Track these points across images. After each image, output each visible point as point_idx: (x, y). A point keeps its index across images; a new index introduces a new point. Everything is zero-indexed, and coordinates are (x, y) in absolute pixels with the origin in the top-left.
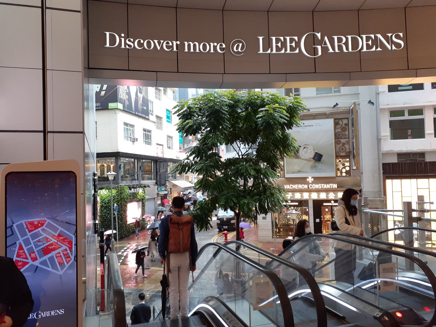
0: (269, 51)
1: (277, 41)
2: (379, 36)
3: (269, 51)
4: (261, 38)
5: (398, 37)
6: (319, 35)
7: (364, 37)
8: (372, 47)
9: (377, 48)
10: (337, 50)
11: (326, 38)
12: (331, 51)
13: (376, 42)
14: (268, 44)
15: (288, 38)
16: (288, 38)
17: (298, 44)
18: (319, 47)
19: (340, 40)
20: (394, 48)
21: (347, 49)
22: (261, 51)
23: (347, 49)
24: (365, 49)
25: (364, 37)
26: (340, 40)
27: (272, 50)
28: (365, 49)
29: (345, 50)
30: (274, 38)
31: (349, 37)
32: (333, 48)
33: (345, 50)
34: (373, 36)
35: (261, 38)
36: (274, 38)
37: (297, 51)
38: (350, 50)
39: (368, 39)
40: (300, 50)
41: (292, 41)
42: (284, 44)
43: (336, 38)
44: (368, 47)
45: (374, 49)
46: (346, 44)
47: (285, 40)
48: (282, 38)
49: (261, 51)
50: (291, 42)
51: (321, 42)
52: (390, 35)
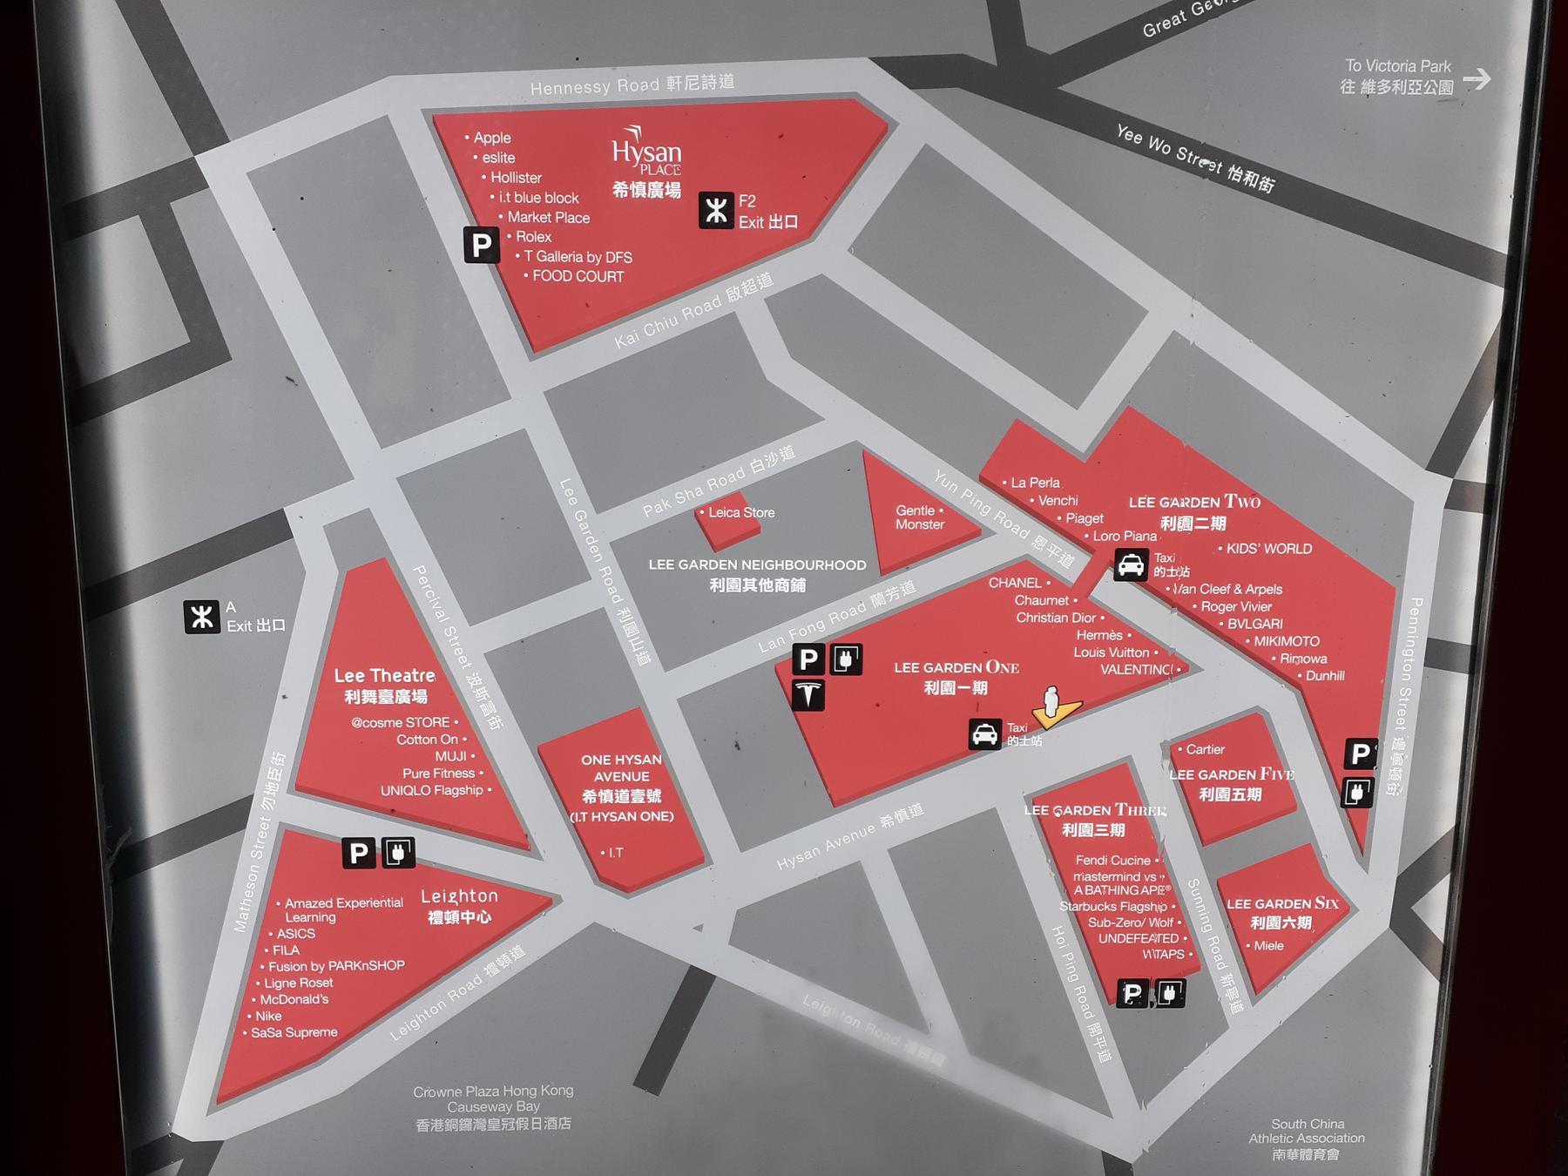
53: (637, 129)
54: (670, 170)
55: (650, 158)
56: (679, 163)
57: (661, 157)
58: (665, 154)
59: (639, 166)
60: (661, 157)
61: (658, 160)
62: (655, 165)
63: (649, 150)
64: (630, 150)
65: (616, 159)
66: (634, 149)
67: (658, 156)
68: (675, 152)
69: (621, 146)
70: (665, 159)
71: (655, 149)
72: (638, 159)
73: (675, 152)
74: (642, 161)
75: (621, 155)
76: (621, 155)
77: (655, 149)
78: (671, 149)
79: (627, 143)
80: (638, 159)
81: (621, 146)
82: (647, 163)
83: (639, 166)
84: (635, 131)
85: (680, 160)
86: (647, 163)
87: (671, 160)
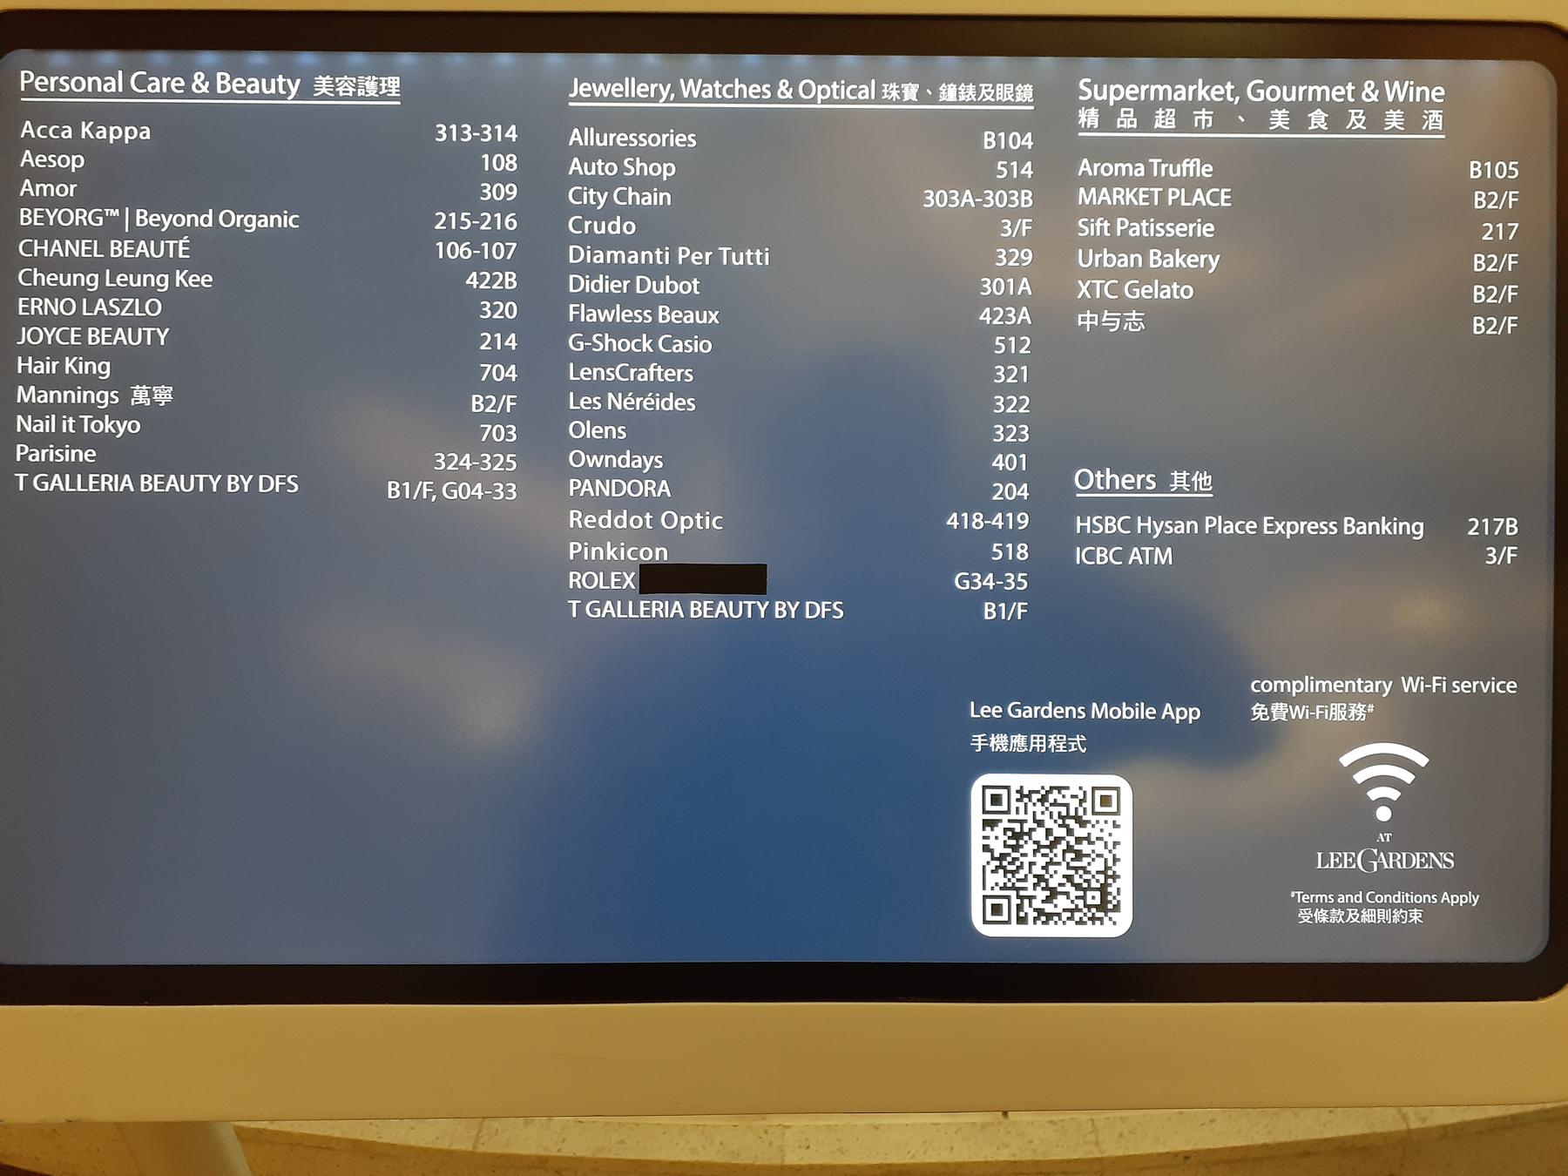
0: (1327, 867)
1: (1335, 856)
2: (1432, 855)
3: (1327, 867)
4: (1320, 854)
5: (1448, 856)
6: (1375, 851)
7: (1418, 854)
10: (1391, 867)
11: (1382, 854)
12: (1386, 867)
13: (1427, 860)
14: (1326, 860)
16: (1346, 854)
17: (1355, 860)
18: (1375, 863)
20: (1445, 867)
22: (1320, 867)
24: (1418, 867)
25: (1418, 854)
28: (1418, 867)
29: (1399, 866)
30: (1332, 854)
31: (1404, 854)
33: (1399, 866)
34: (1426, 854)
35: (1320, 854)
36: (1332, 854)
38: (1404, 867)
40: (1357, 865)
41: (1349, 857)
42: (1342, 860)
43: (1391, 854)
46: (1401, 861)
47: (1343, 855)
48: (1340, 854)
49: (1320, 867)
52: (1441, 854)
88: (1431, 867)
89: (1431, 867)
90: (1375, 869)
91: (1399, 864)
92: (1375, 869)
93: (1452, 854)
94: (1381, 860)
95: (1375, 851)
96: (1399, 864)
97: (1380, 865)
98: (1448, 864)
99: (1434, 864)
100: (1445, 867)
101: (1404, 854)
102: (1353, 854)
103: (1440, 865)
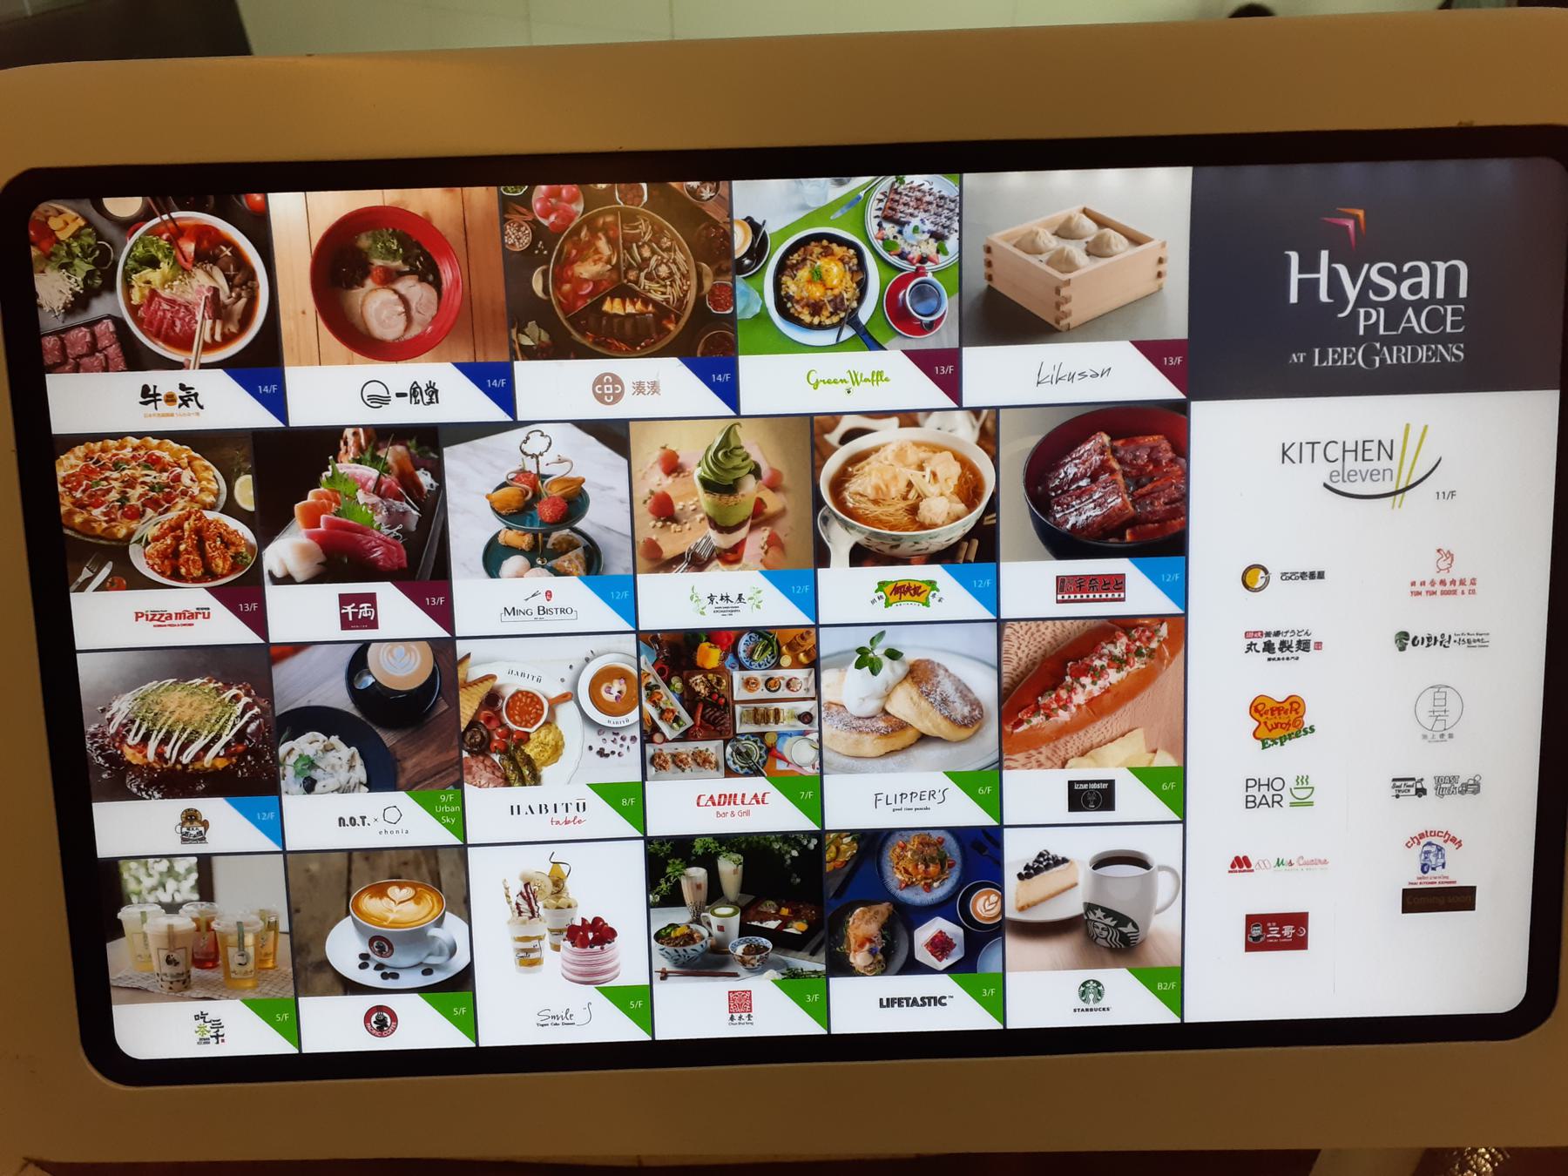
0: (1325, 364)
2: (1440, 347)
3: (1325, 364)
5: (1458, 348)
6: (1378, 345)
8: (1432, 359)
9: (1436, 359)
10: (1395, 361)
11: (1385, 349)
13: (1435, 353)
14: (1323, 357)
15: (1345, 350)
16: (1345, 350)
17: (1355, 356)
18: (1377, 359)
19: (1399, 351)
20: (1453, 360)
21: (1406, 360)
23: (1406, 360)
24: (1424, 361)
25: (1425, 347)
26: (1399, 351)
27: (1328, 363)
28: (1424, 361)
29: (1403, 361)
30: (1330, 350)
31: (1409, 348)
32: (1392, 360)
36: (1330, 350)
37: (1354, 363)
38: (1409, 361)
39: (1428, 350)
40: (1357, 362)
42: (1341, 357)
43: (1395, 348)
44: (1428, 358)
45: (1433, 360)
46: (1406, 355)
47: (1342, 351)
49: (1316, 364)
50: (1348, 353)
51: (1379, 353)
52: (1450, 346)
53: (1356, 218)
54: (1435, 320)
55: (1384, 291)
56: (1462, 301)
57: (1415, 289)
58: (1425, 279)
59: (1354, 314)
60: (1415, 289)
61: (1405, 295)
62: (1395, 309)
63: (1382, 272)
64: (1334, 276)
65: (1294, 298)
66: (1342, 270)
67: (1406, 285)
68: (1452, 274)
69: (1309, 264)
70: (1425, 293)
71: (1400, 268)
72: (1352, 293)
73: (1452, 274)
74: (1362, 300)
75: (1308, 288)
76: (1308, 288)
77: (1400, 268)
78: (1441, 267)
79: (1324, 255)
80: (1352, 293)
81: (1309, 264)
82: (1376, 305)
83: (1354, 314)
84: (1350, 224)
85: (1463, 293)
86: (1376, 305)
87: (1440, 294)
88: (1438, 361)
89: (1438, 361)
90: (1377, 365)
91: (1403, 358)
92: (1377, 365)
93: (1462, 346)
94: (1384, 354)
95: (1378, 345)
96: (1403, 358)
97: (1383, 361)
98: (1457, 357)
99: (1442, 356)
100: (1453, 360)
101: (1409, 348)
102: (1354, 349)
103: (1449, 358)
